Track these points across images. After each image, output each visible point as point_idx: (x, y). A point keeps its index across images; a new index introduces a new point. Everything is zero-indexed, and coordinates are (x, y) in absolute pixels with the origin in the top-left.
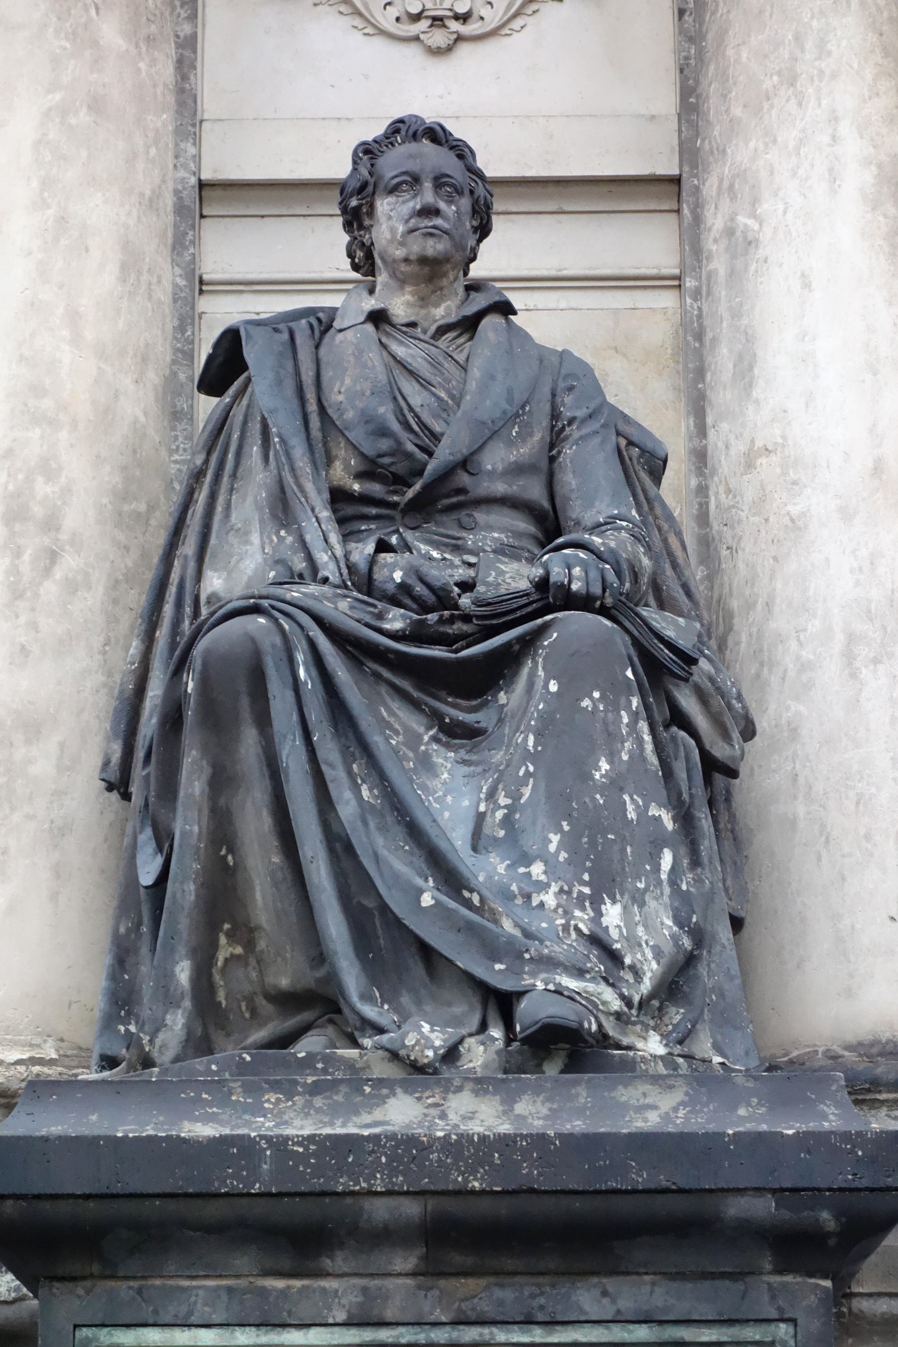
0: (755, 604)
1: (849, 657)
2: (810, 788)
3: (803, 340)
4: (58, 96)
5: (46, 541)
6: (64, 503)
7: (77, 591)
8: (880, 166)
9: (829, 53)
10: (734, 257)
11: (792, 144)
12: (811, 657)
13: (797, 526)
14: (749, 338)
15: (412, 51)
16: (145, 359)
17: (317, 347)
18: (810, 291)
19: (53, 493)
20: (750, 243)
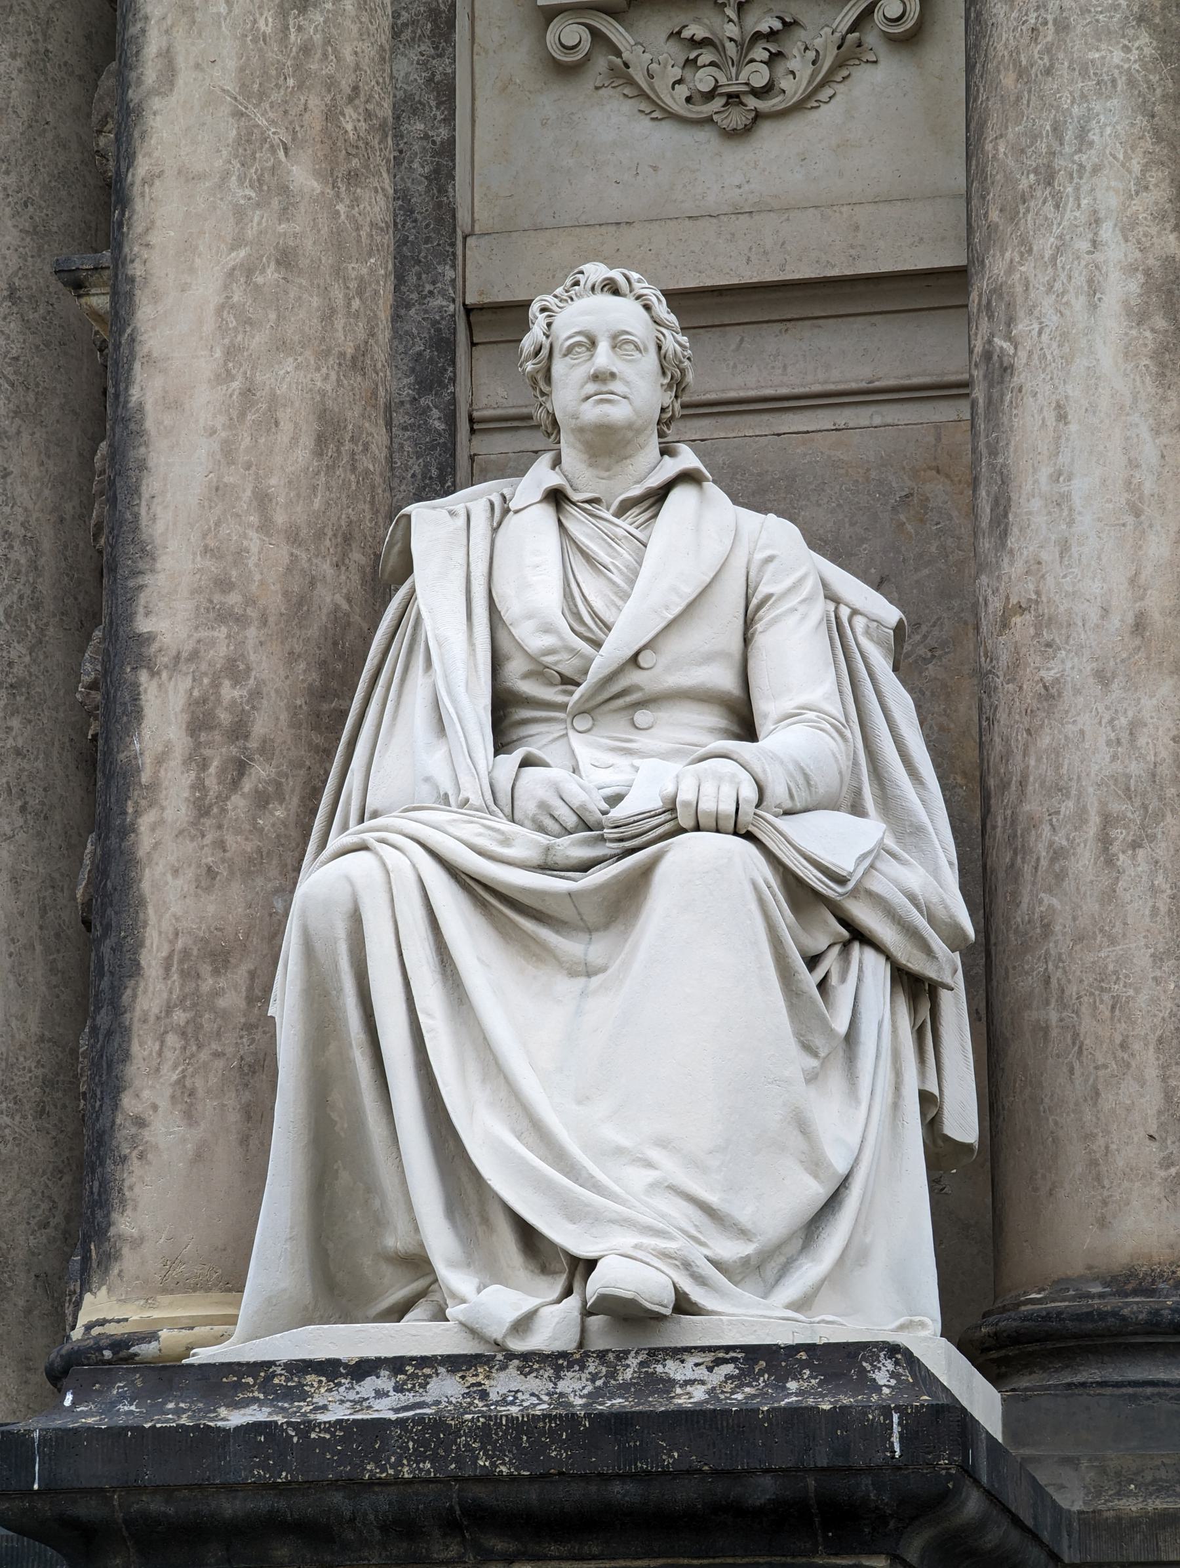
0: (1009, 783)
1: (1105, 841)
2: (1063, 991)
3: (1058, 481)
4: (242, 253)
5: (234, 751)
6: (253, 708)
7: (267, 803)
8: (1148, 273)
9: (1091, 144)
10: (991, 385)
11: (1048, 254)
12: (1064, 843)
13: (1050, 694)
14: (1005, 481)
15: (704, 135)
16: (347, 539)
17: (495, 530)
18: (1066, 424)
19: (241, 697)
20: (1005, 370)
